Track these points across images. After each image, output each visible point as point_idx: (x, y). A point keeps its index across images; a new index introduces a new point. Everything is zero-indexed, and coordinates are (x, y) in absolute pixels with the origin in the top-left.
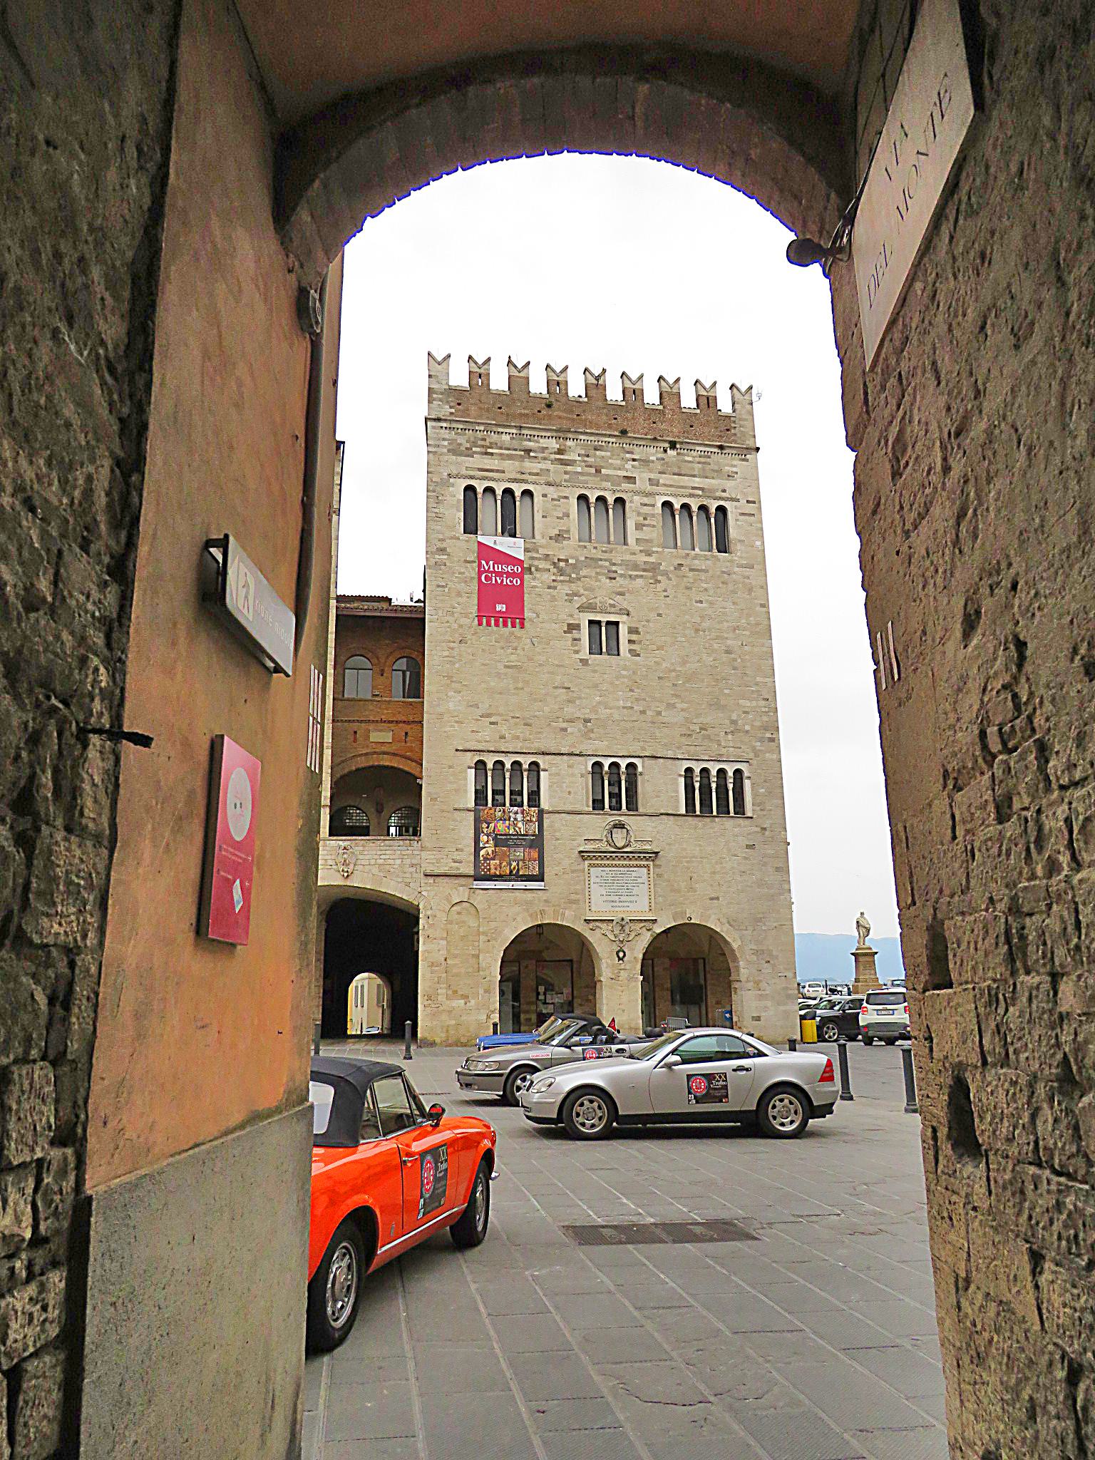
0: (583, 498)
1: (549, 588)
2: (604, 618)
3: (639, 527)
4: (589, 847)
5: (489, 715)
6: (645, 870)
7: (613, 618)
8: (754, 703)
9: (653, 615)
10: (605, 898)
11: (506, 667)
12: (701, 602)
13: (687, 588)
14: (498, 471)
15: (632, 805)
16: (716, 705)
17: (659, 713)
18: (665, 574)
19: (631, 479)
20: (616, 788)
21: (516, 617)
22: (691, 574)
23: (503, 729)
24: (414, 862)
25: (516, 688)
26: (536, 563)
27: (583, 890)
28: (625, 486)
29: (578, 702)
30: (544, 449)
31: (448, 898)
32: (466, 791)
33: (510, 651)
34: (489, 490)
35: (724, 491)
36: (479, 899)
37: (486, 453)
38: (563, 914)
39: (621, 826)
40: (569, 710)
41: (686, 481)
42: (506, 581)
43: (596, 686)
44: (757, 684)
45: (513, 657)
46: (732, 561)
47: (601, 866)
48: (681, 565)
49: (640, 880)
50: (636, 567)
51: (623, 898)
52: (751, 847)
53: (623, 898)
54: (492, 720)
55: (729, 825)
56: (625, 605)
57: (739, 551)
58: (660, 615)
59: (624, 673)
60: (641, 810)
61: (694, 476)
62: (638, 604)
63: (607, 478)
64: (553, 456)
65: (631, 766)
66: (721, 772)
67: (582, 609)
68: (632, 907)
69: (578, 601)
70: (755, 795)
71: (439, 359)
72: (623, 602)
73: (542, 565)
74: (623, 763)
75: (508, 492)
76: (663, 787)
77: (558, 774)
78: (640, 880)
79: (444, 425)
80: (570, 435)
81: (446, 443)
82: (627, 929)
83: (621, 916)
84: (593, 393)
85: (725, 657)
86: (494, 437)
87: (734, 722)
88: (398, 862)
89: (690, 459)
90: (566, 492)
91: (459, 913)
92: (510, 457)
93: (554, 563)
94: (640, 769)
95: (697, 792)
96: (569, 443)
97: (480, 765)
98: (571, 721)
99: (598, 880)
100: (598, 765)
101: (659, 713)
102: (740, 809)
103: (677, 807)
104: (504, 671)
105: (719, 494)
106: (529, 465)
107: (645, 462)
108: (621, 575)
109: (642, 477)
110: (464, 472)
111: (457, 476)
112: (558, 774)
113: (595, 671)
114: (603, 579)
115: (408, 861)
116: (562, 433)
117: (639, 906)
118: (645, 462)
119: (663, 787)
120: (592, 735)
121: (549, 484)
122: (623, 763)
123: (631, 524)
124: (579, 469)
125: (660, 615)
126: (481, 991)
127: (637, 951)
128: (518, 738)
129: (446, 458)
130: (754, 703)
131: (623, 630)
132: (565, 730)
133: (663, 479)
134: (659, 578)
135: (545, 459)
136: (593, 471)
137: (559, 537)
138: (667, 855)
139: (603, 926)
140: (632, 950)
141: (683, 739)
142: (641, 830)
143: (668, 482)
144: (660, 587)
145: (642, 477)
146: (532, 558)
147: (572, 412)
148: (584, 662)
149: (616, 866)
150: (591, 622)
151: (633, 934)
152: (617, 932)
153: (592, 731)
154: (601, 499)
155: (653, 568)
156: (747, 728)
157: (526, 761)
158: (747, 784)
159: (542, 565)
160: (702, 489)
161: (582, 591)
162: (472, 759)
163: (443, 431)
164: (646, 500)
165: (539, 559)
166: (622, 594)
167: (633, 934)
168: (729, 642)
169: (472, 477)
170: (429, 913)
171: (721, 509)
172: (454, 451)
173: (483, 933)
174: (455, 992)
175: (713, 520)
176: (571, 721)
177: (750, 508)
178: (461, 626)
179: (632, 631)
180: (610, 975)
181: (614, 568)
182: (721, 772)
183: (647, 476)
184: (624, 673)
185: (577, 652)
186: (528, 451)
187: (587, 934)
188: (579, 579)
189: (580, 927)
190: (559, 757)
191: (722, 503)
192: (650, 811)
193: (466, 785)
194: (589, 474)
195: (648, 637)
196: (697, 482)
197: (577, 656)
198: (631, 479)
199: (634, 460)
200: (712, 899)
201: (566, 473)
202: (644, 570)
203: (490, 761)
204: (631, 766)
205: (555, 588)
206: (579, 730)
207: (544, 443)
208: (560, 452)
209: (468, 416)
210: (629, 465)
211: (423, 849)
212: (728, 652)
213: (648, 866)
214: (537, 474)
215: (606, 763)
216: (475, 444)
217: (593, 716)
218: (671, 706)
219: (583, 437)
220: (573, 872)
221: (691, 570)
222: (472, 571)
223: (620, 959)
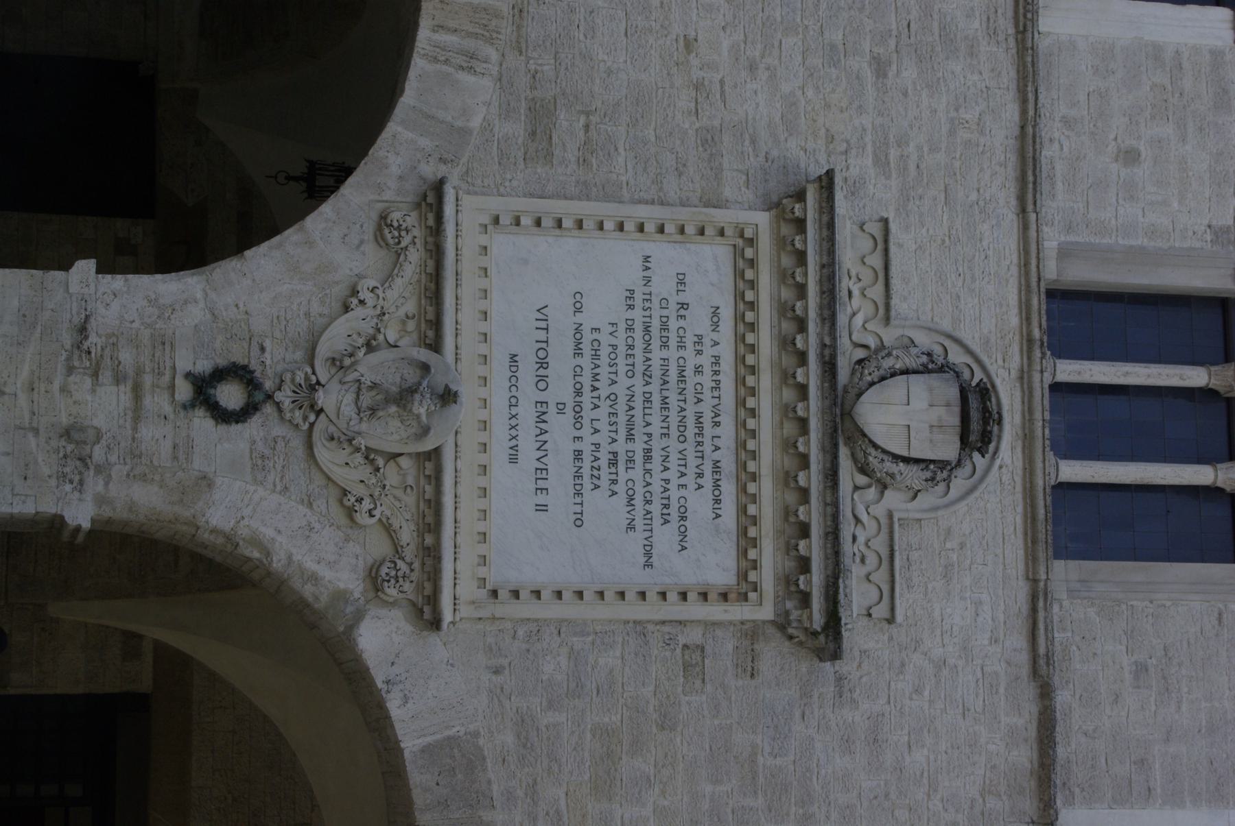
6: (719, 568)
10: (562, 321)
15: (1083, 526)
27: (610, 194)
39: (977, 421)
47: (745, 304)
49: (665, 537)
51: (560, 426)
53: (560, 426)
60: (1064, 572)
68: (510, 484)
78: (665, 537)
82: (388, 432)
83: (468, 392)
99: (663, 285)
117: (528, 521)
139: (402, 297)
142: (954, 565)
149: (745, 392)
152: (369, 367)
167: (352, 474)
180: (107, 317)
187: (355, 198)
189: (398, 155)
213: (744, 588)
220: (709, 140)
223: (203, 390)
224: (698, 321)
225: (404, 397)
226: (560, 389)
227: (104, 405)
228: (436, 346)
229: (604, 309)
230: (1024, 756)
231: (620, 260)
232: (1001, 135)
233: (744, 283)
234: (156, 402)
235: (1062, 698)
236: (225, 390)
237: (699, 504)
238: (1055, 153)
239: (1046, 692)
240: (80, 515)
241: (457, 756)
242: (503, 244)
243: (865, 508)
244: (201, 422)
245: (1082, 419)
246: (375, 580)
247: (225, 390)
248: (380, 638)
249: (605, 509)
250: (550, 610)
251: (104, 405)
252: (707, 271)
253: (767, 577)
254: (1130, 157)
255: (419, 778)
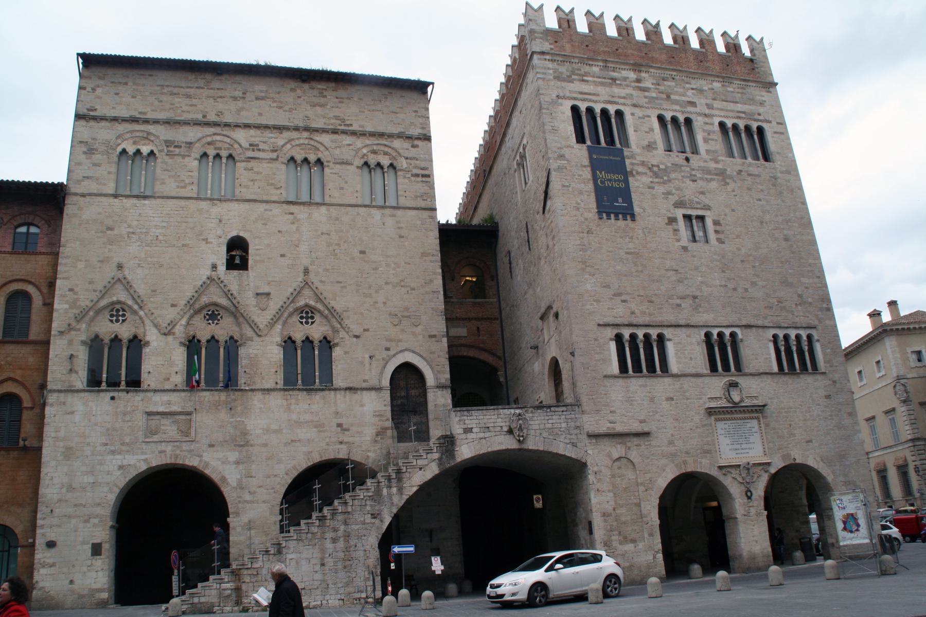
0: (661, 118)
1: (649, 188)
2: (694, 213)
3: (706, 140)
4: (713, 405)
5: (619, 295)
6: (755, 422)
7: (700, 213)
8: (811, 281)
9: (727, 211)
10: (731, 447)
11: (627, 253)
12: (760, 200)
13: (749, 189)
14: (594, 94)
15: (738, 368)
16: (785, 283)
17: (746, 290)
18: (731, 178)
19: (693, 104)
20: (722, 353)
21: (628, 213)
22: (749, 178)
23: (633, 306)
24: (578, 424)
25: (637, 271)
26: (636, 168)
27: (713, 441)
28: (690, 109)
29: (686, 282)
30: (625, 79)
31: (609, 455)
32: (610, 360)
33: (627, 239)
34: (590, 110)
35: (759, 114)
36: (634, 455)
37: (583, 80)
38: (701, 463)
39: (734, 385)
40: (681, 289)
41: (731, 106)
42: (615, 185)
43: (697, 268)
44: (810, 265)
45: (631, 246)
46: (775, 168)
47: (727, 419)
48: (741, 171)
50: (709, 172)
51: (744, 446)
52: (828, 397)
53: (744, 446)
54: (623, 298)
55: (807, 381)
56: (707, 201)
57: (778, 162)
58: (733, 210)
59: (715, 257)
61: (737, 102)
62: (718, 201)
63: (676, 102)
64: (633, 84)
65: (733, 335)
66: (798, 337)
67: (679, 204)
69: (673, 199)
70: (824, 354)
71: (536, 7)
72: (705, 200)
73: (640, 169)
74: (727, 332)
75: (604, 112)
76: (758, 352)
77: (680, 343)
78: (754, 430)
79: (548, 57)
80: (643, 69)
81: (551, 72)
82: (751, 471)
83: (745, 461)
84: (653, 37)
85: (784, 244)
86: (587, 69)
87: (800, 296)
88: (564, 425)
89: (731, 89)
90: (649, 112)
91: (619, 468)
92: (602, 84)
93: (649, 168)
94: (740, 336)
95: (783, 354)
96: (643, 75)
97: (619, 338)
98: (683, 298)
99: (723, 432)
100: (708, 335)
101: (746, 290)
102: (815, 367)
103: (771, 366)
104: (625, 256)
105: (756, 117)
106: (616, 91)
107: (700, 91)
108: (701, 179)
109: (701, 102)
110: (568, 94)
111: (564, 98)
112: (680, 343)
113: (694, 256)
114: (688, 182)
115: (572, 424)
116: (637, 67)
118: (700, 91)
119: (758, 352)
120: (700, 309)
121: (635, 106)
122: (727, 332)
123: (699, 137)
124: (654, 95)
125: (733, 210)
126: (646, 535)
127: (759, 490)
128: (644, 313)
129: (552, 83)
130: (811, 281)
131: (709, 222)
132: (679, 305)
133: (716, 104)
134: (728, 181)
135: (628, 86)
136: (664, 96)
137: (650, 147)
138: (772, 407)
139: (733, 471)
140: (756, 489)
141: (767, 311)
143: (719, 107)
144: (729, 188)
145: (701, 102)
146: (632, 164)
147: (641, 51)
148: (685, 249)
149: (735, 419)
150: (685, 216)
151: (756, 476)
153: (700, 306)
154: (674, 120)
155: (722, 173)
156: (810, 300)
157: (654, 333)
158: (818, 347)
159: (640, 169)
160: (744, 113)
161: (674, 191)
162: (610, 333)
163: (547, 62)
164: (706, 120)
165: (638, 165)
166: (703, 193)
167: (756, 476)
168: (785, 232)
169: (575, 99)
170: (596, 469)
171: (760, 130)
172: (558, 78)
173: (641, 484)
174: (625, 538)
175: (756, 137)
176: (683, 298)
177: (779, 129)
178: (586, 219)
179: (716, 223)
180: (743, 512)
181: (694, 173)
182: (798, 337)
183: (703, 101)
184: (715, 257)
185: (678, 240)
186: (614, 80)
187: (721, 478)
188: (669, 181)
189: (714, 472)
190: (678, 331)
191: (760, 124)
192: (754, 371)
193: (610, 355)
194: (662, 99)
195: (728, 228)
196: (739, 107)
197: (679, 244)
198: (693, 104)
199: (693, 89)
200: (808, 442)
201: (646, 97)
202: (716, 175)
203: (626, 333)
204: (733, 335)
205: (653, 188)
206: (691, 306)
207: (625, 73)
208: (638, 81)
209: (564, 50)
210: (690, 93)
211: (583, 412)
212: (786, 239)
213: (758, 418)
214: (624, 98)
215: (715, 332)
216: (573, 73)
217: (698, 293)
218: (753, 284)
219: (651, 70)
220: (703, 426)
221: (750, 175)
222: (587, 173)
223: (749, 498)
224: (726, 426)
225: (748, 469)
226: (738, 446)
227: (753, 511)
228: (739, 466)
229: (728, 441)
230: (769, 377)
231: (721, 438)
232: (693, 379)
233: (722, 420)
234: (751, 504)
235: (761, 371)
236: (749, 495)
237: (749, 425)
238: (694, 371)
239: (762, 373)
240: (766, 513)
241: (784, 457)
242: (723, 456)
243: (747, 402)
244: (753, 497)
245: (726, 368)
246: (766, 472)
247: (749, 495)
248: (773, 470)
249: (752, 439)
250: (766, 446)
251: (753, 511)
252: (721, 425)
253: (756, 415)
254: (691, 359)
255: (787, 463)
